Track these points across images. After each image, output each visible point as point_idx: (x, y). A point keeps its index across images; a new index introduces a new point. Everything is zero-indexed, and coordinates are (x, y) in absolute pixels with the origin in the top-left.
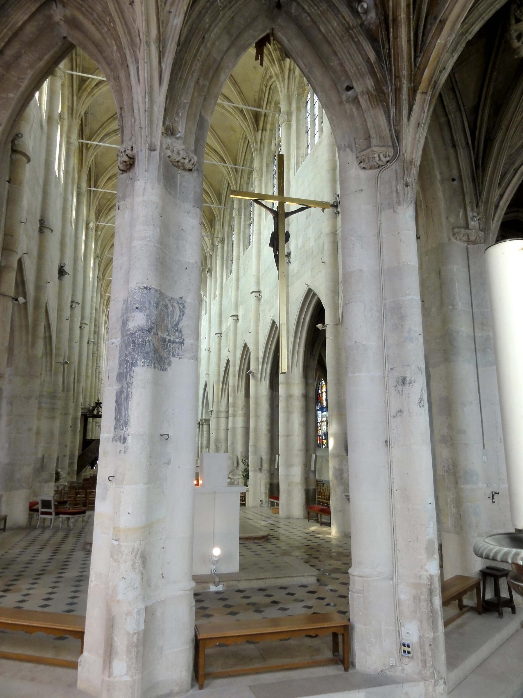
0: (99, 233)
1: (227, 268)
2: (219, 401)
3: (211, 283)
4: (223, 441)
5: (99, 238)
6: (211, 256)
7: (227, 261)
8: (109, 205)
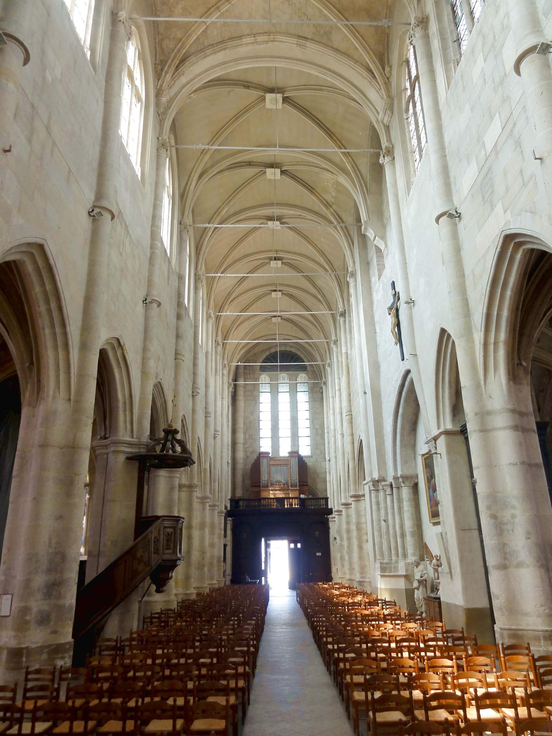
0: (164, 100)
1: (446, 62)
2: (478, 386)
3: (394, 173)
4: (515, 503)
5: (165, 113)
6: (387, 128)
7: (444, 49)
8: (179, 51)
